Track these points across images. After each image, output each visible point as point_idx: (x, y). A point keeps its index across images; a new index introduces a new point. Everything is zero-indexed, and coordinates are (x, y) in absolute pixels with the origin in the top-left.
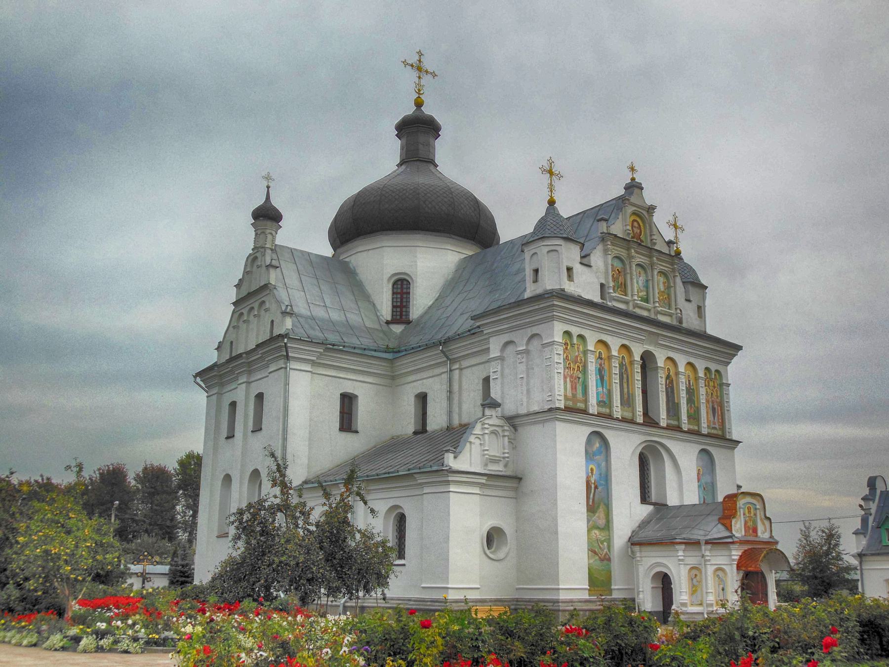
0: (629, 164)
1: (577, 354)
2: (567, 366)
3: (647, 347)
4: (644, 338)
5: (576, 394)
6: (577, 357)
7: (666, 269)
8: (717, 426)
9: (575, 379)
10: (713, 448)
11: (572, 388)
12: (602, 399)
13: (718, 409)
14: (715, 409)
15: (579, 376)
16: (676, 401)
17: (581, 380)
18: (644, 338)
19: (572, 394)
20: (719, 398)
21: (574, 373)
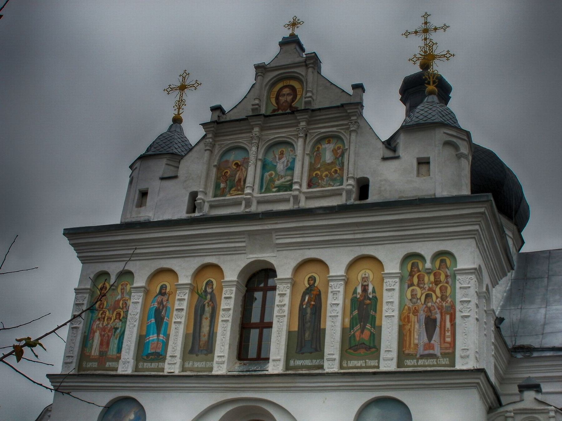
0: (300, 17)
1: (119, 297)
2: (100, 316)
3: (251, 256)
4: (243, 244)
5: (107, 352)
6: (118, 301)
7: (334, 129)
8: (437, 351)
9: (109, 331)
10: (406, 392)
11: (101, 344)
12: (153, 351)
13: (443, 320)
14: (435, 320)
15: (118, 326)
16: (322, 327)
17: (118, 331)
18: (243, 244)
19: (100, 352)
20: (523, 300)
21: (108, 324)
